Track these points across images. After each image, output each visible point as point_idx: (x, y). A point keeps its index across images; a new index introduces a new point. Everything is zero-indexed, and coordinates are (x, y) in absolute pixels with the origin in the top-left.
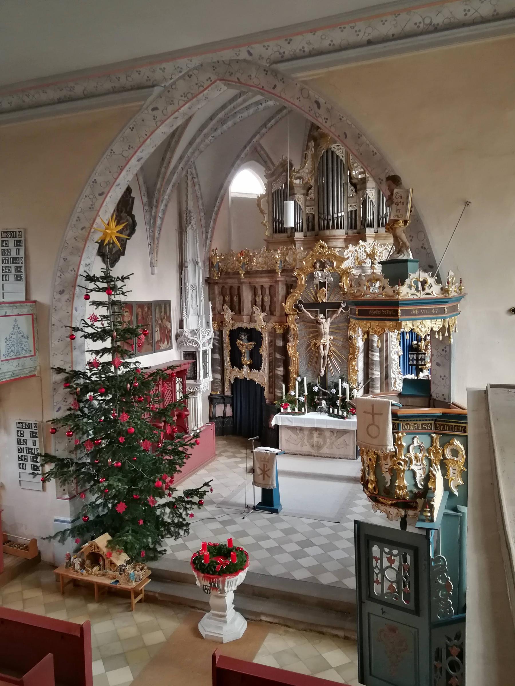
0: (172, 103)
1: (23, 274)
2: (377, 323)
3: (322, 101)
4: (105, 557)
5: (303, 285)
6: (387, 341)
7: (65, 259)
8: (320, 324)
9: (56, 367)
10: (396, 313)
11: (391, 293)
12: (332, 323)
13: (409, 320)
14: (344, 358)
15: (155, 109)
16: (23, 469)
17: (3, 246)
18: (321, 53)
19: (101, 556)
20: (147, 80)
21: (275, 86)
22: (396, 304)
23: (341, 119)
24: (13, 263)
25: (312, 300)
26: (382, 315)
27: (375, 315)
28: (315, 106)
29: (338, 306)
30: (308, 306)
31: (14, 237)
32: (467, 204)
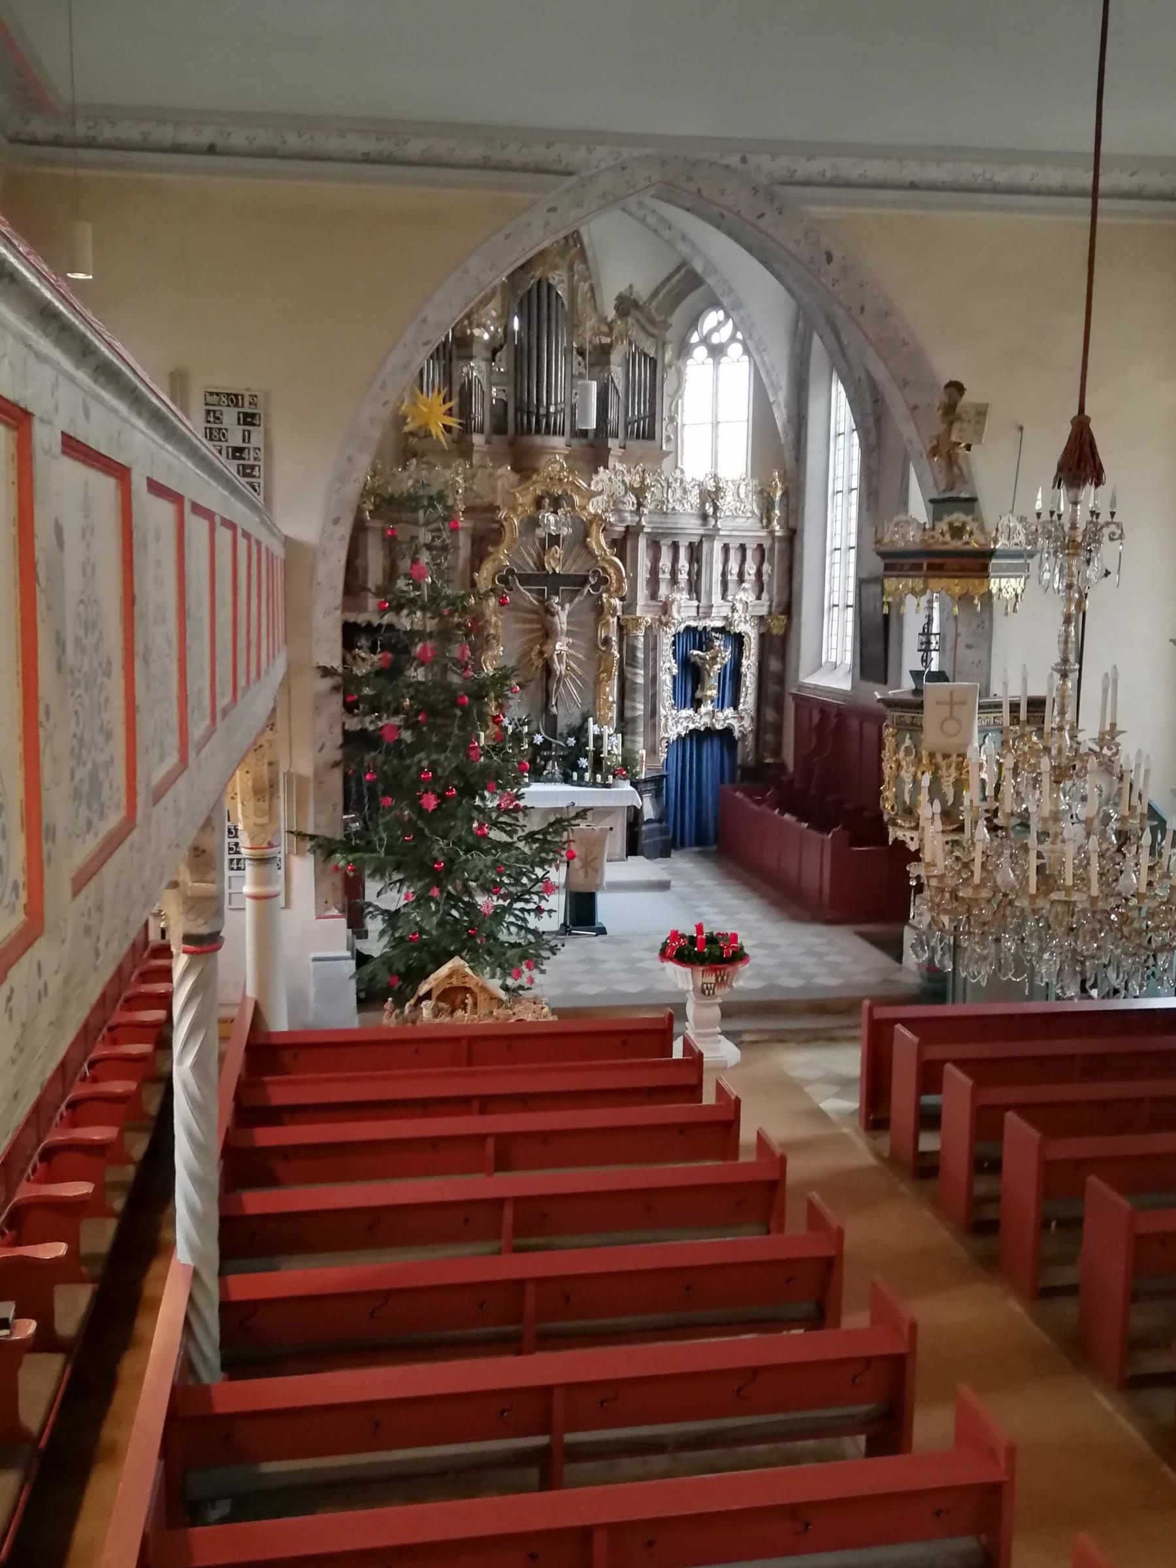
0: (580, 205)
1: (261, 481)
2: (956, 581)
3: (837, 254)
4: (477, 990)
5: (514, 541)
6: (655, 648)
7: (349, 459)
8: (553, 615)
9: (321, 664)
10: (985, 568)
11: (982, 541)
12: (570, 615)
13: (1005, 577)
14: (587, 678)
15: (553, 210)
16: (239, 869)
17: (209, 422)
18: (848, 184)
19: (467, 990)
20: (554, 161)
21: (763, 215)
22: (991, 554)
23: (861, 286)
24: (234, 457)
25: (530, 567)
26: (963, 569)
27: (952, 570)
28: (824, 257)
29: (584, 581)
30: (526, 580)
31: (237, 405)
32: (1021, 429)
